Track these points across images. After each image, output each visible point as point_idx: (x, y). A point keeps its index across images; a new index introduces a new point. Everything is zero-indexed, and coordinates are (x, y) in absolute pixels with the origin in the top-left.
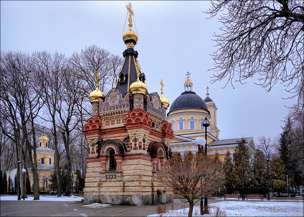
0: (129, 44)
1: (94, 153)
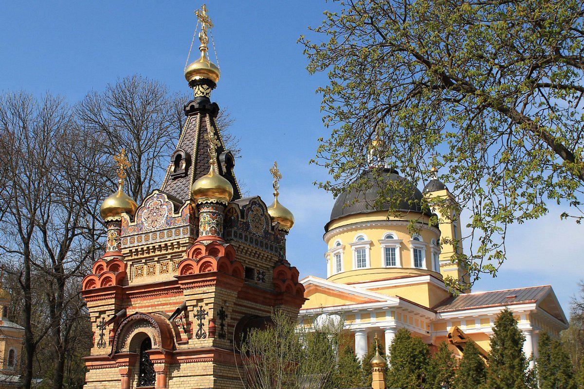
0: (199, 89)
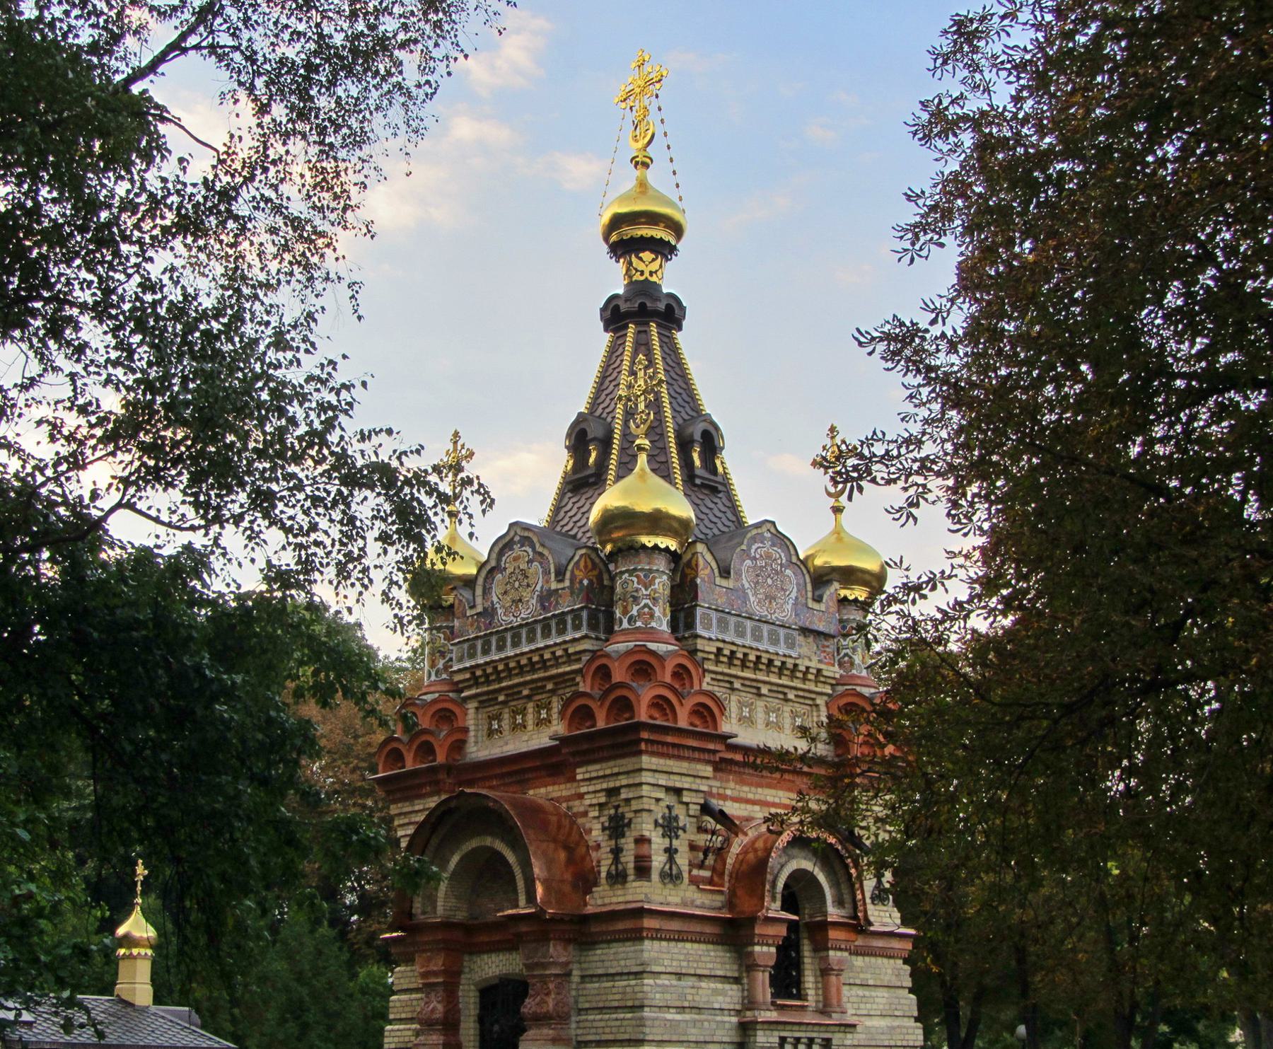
1: (679, 876)
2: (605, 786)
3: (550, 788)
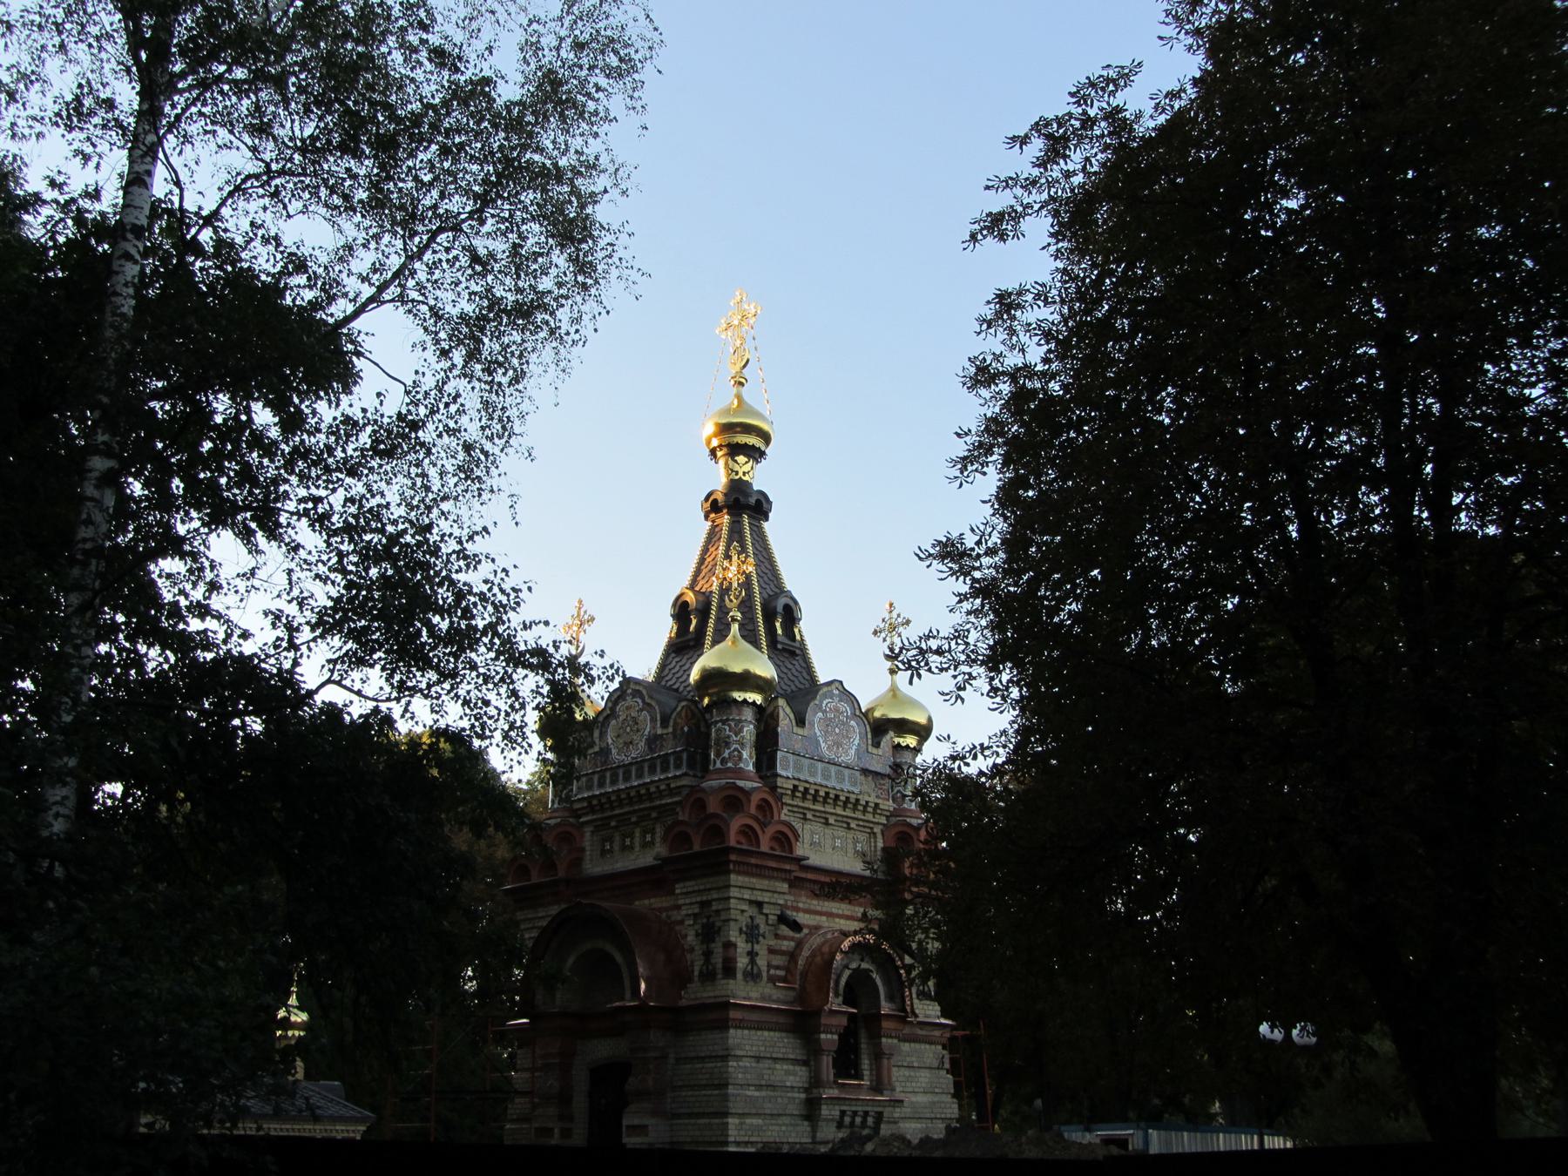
2: (699, 899)
3: (652, 900)
